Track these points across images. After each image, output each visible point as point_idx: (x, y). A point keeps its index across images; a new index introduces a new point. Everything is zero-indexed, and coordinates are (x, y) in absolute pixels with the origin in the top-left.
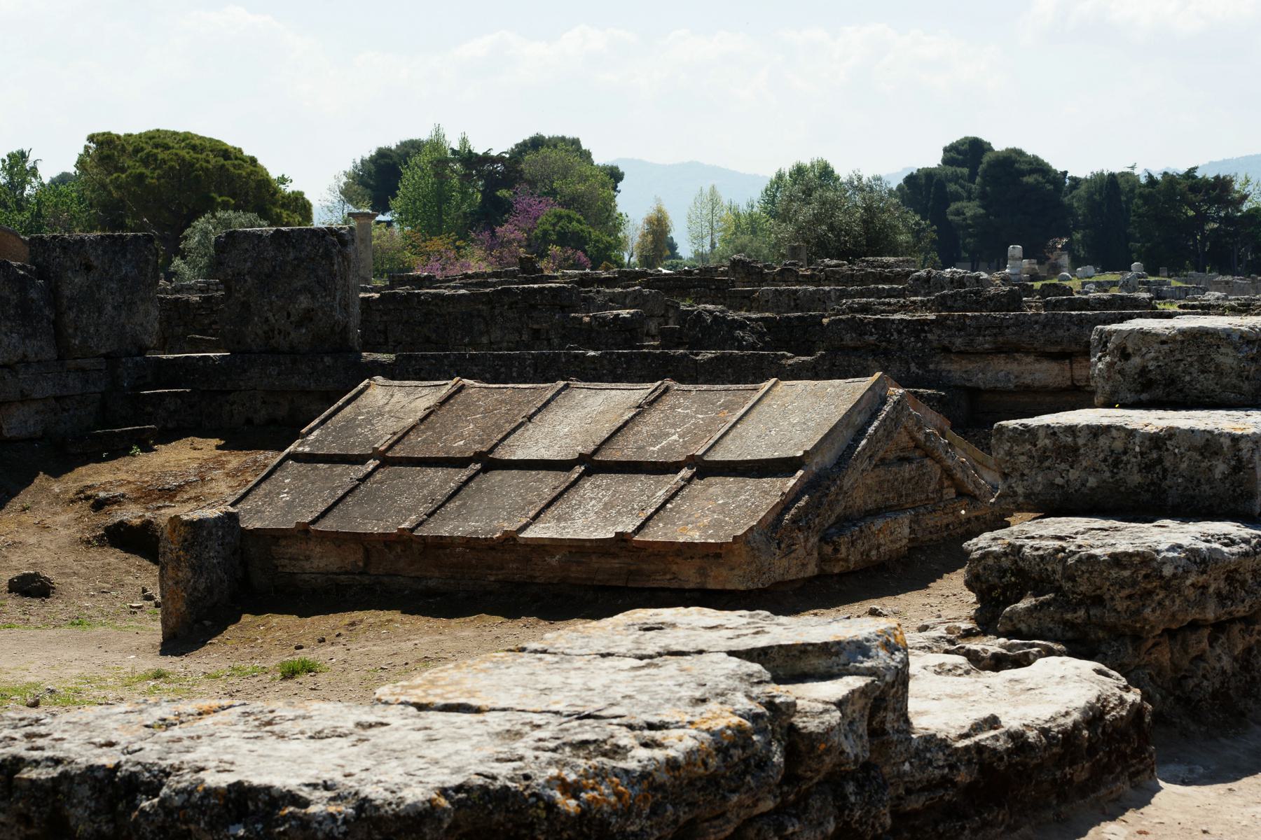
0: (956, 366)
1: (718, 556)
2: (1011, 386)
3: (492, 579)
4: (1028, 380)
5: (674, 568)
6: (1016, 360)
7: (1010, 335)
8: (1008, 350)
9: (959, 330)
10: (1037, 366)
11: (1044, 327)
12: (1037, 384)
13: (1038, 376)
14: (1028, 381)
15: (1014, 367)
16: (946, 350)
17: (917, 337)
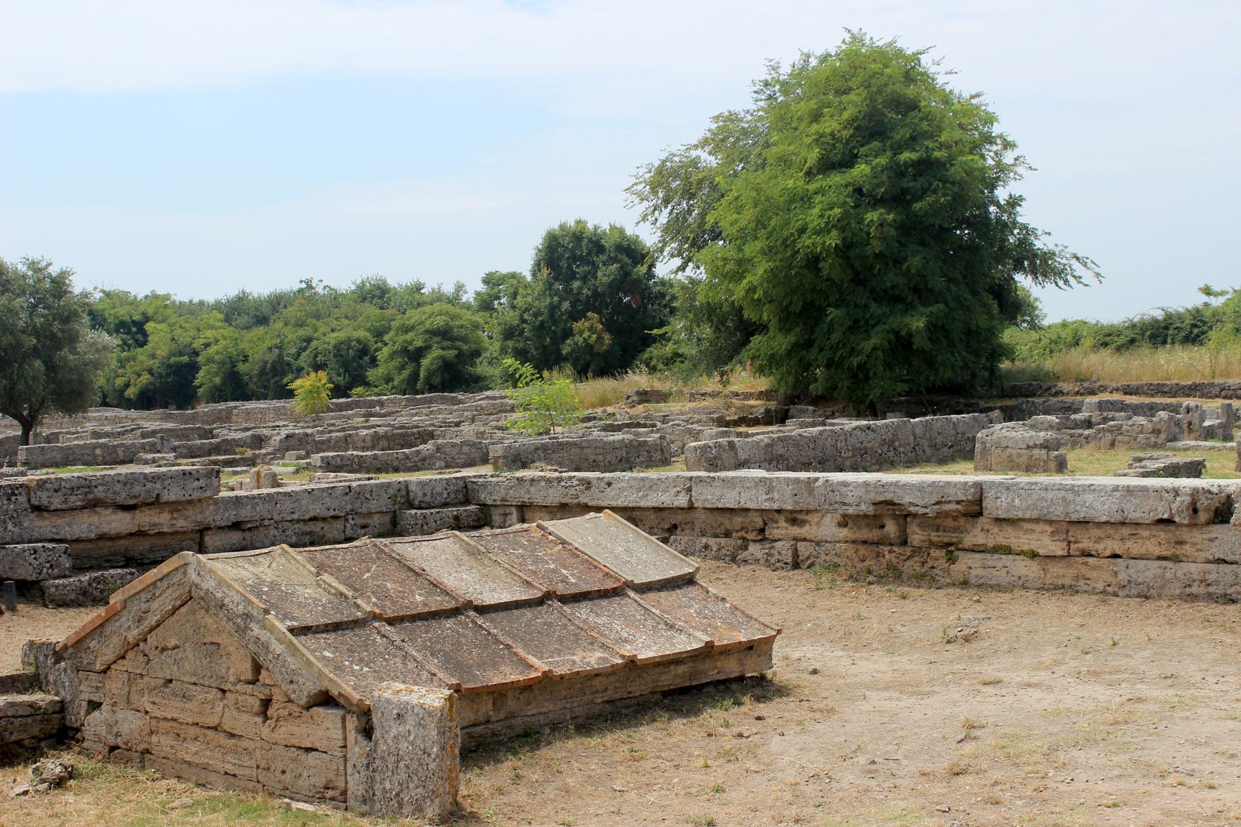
0: (46, 522)
1: (751, 648)
2: (93, 536)
3: (599, 701)
4: (106, 529)
5: (719, 664)
6: (97, 513)
7: (99, 492)
8: (93, 505)
9: (56, 491)
10: (113, 517)
11: (125, 484)
12: (113, 532)
13: (114, 525)
14: (106, 530)
15: (95, 519)
16: (38, 509)
17: (9, 499)
